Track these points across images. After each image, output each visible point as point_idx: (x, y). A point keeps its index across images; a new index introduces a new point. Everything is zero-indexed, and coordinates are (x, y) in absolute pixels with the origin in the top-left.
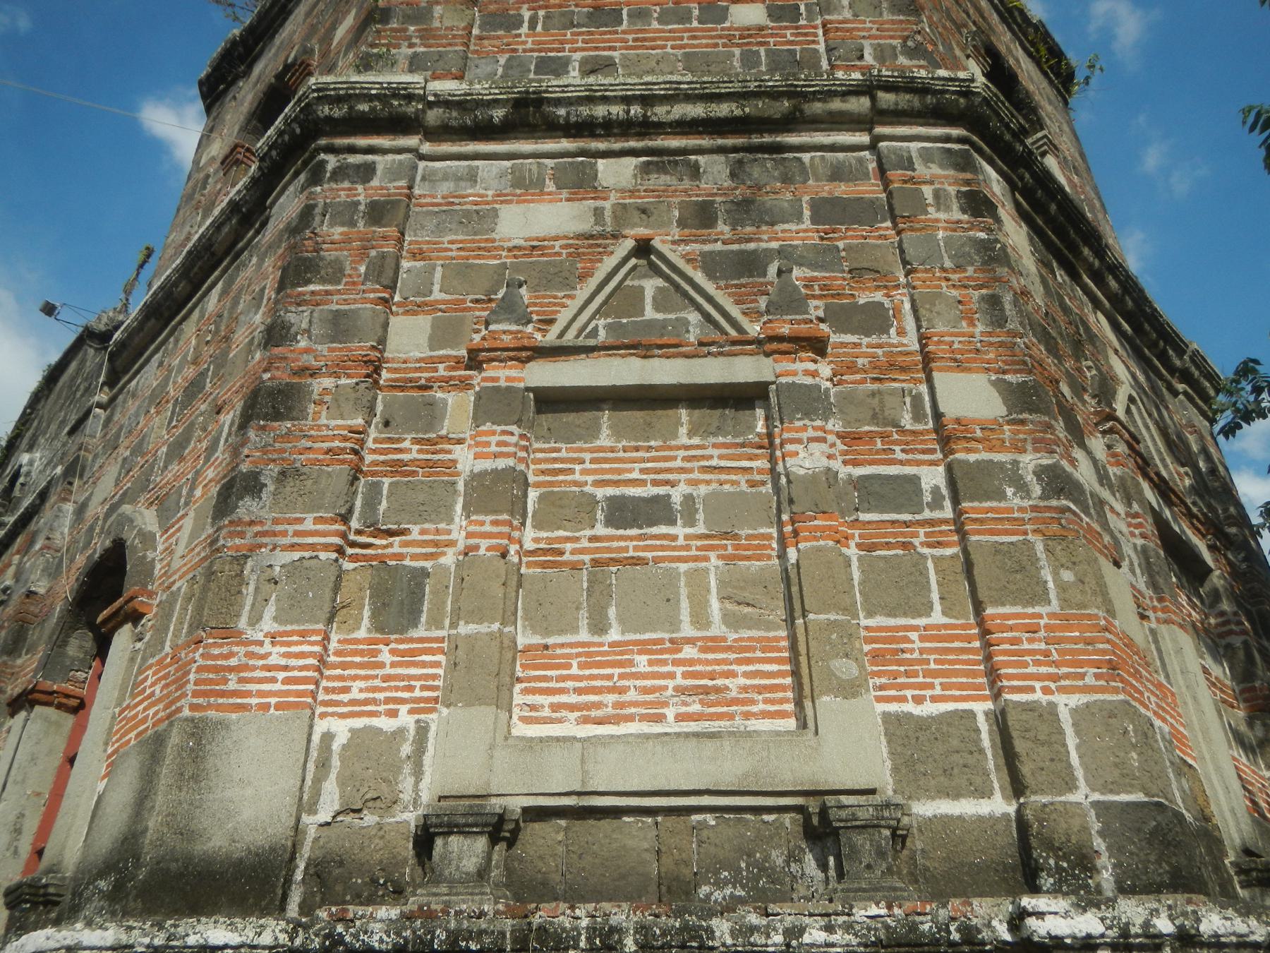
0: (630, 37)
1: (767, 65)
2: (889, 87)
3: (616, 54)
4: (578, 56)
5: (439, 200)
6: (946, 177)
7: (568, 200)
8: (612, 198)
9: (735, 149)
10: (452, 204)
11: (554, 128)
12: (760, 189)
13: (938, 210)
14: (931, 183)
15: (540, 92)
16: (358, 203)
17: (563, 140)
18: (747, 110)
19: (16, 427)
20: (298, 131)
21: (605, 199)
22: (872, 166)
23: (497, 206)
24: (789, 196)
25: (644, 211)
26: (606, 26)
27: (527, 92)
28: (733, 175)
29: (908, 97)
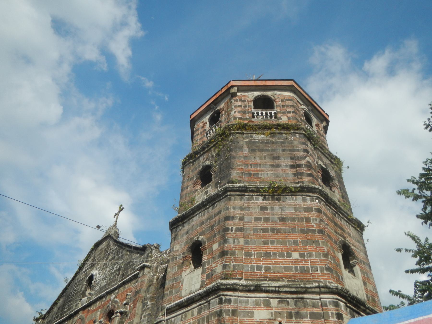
0: (273, 261)
1: (300, 271)
2: (323, 287)
3: (271, 266)
4: (264, 266)
5: (243, 308)
6: (333, 309)
7: (266, 309)
8: (274, 310)
9: (295, 298)
10: (245, 309)
11: (262, 291)
12: (300, 309)
13: (332, 318)
14: (330, 310)
15: (260, 285)
16: (229, 310)
17: (264, 293)
18: (297, 290)
19: (86, 258)
20: (216, 288)
21: (272, 310)
22: (320, 304)
23: (253, 310)
24: (305, 311)
25: (280, 313)
26: (268, 257)
27: (258, 284)
28: (295, 305)
29: (326, 289)
